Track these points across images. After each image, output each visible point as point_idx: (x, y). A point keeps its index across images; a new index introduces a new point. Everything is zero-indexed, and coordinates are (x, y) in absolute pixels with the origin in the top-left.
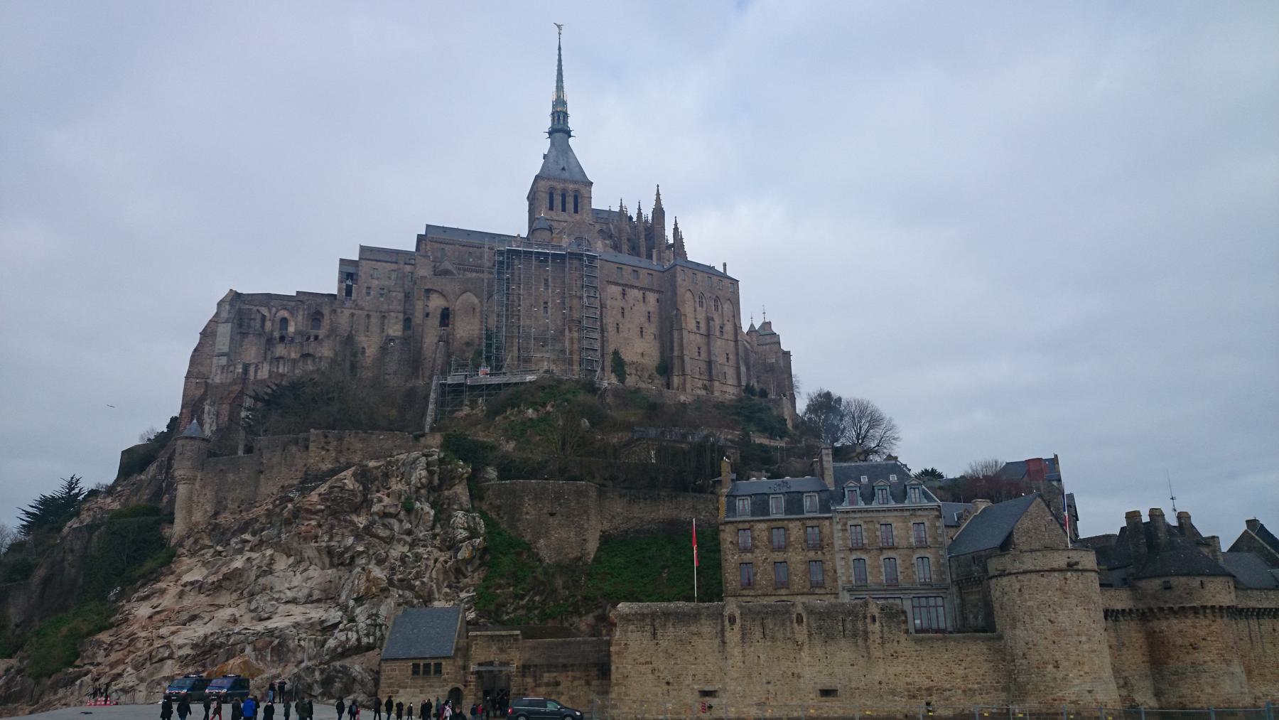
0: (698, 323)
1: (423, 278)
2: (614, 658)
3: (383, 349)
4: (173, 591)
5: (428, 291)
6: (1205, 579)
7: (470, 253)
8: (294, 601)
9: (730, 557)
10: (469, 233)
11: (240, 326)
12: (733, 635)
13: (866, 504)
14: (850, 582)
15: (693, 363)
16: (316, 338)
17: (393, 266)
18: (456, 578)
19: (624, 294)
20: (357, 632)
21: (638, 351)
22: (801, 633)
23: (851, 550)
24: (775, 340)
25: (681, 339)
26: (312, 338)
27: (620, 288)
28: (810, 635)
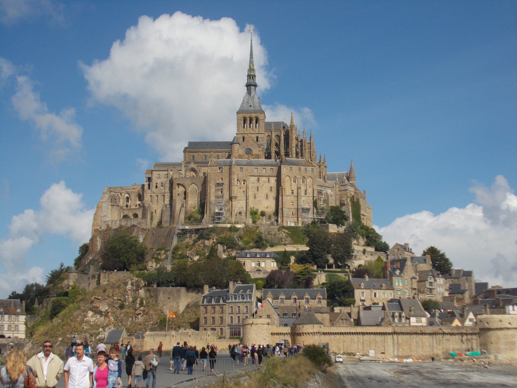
1: (176, 178)
2: (144, 345)
5: (178, 184)
6: (304, 325)
7: (206, 156)
9: (201, 315)
11: (111, 202)
13: (235, 300)
14: (229, 323)
17: (166, 172)
18: (135, 319)
20: (104, 335)
21: (265, 206)
23: (230, 314)
24: (346, 188)
26: (138, 205)
27: (256, 178)
28: (192, 339)
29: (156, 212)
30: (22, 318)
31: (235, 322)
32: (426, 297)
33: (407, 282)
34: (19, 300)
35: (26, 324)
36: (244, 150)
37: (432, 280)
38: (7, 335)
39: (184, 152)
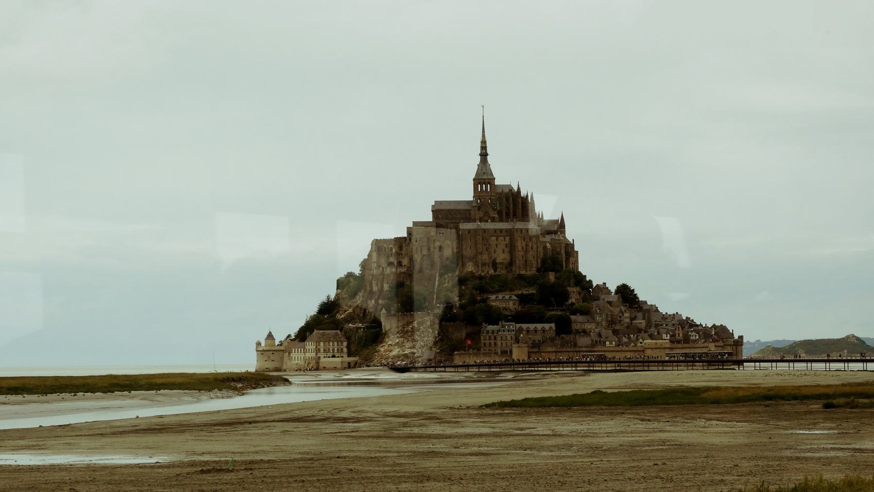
0: (522, 247)
1: (433, 236)
3: (422, 259)
4: (387, 346)
5: (434, 240)
8: (408, 348)
10: (450, 202)
11: (379, 251)
12: (471, 356)
15: (519, 261)
16: (402, 254)
19: (497, 239)
21: (503, 258)
22: (481, 356)
25: (515, 255)
27: (496, 237)
29: (416, 261)
30: (345, 344)
31: (504, 345)
32: (617, 327)
33: (604, 317)
34: (339, 331)
35: (348, 347)
36: (483, 213)
37: (621, 315)
38: (337, 355)
39: (432, 211)
